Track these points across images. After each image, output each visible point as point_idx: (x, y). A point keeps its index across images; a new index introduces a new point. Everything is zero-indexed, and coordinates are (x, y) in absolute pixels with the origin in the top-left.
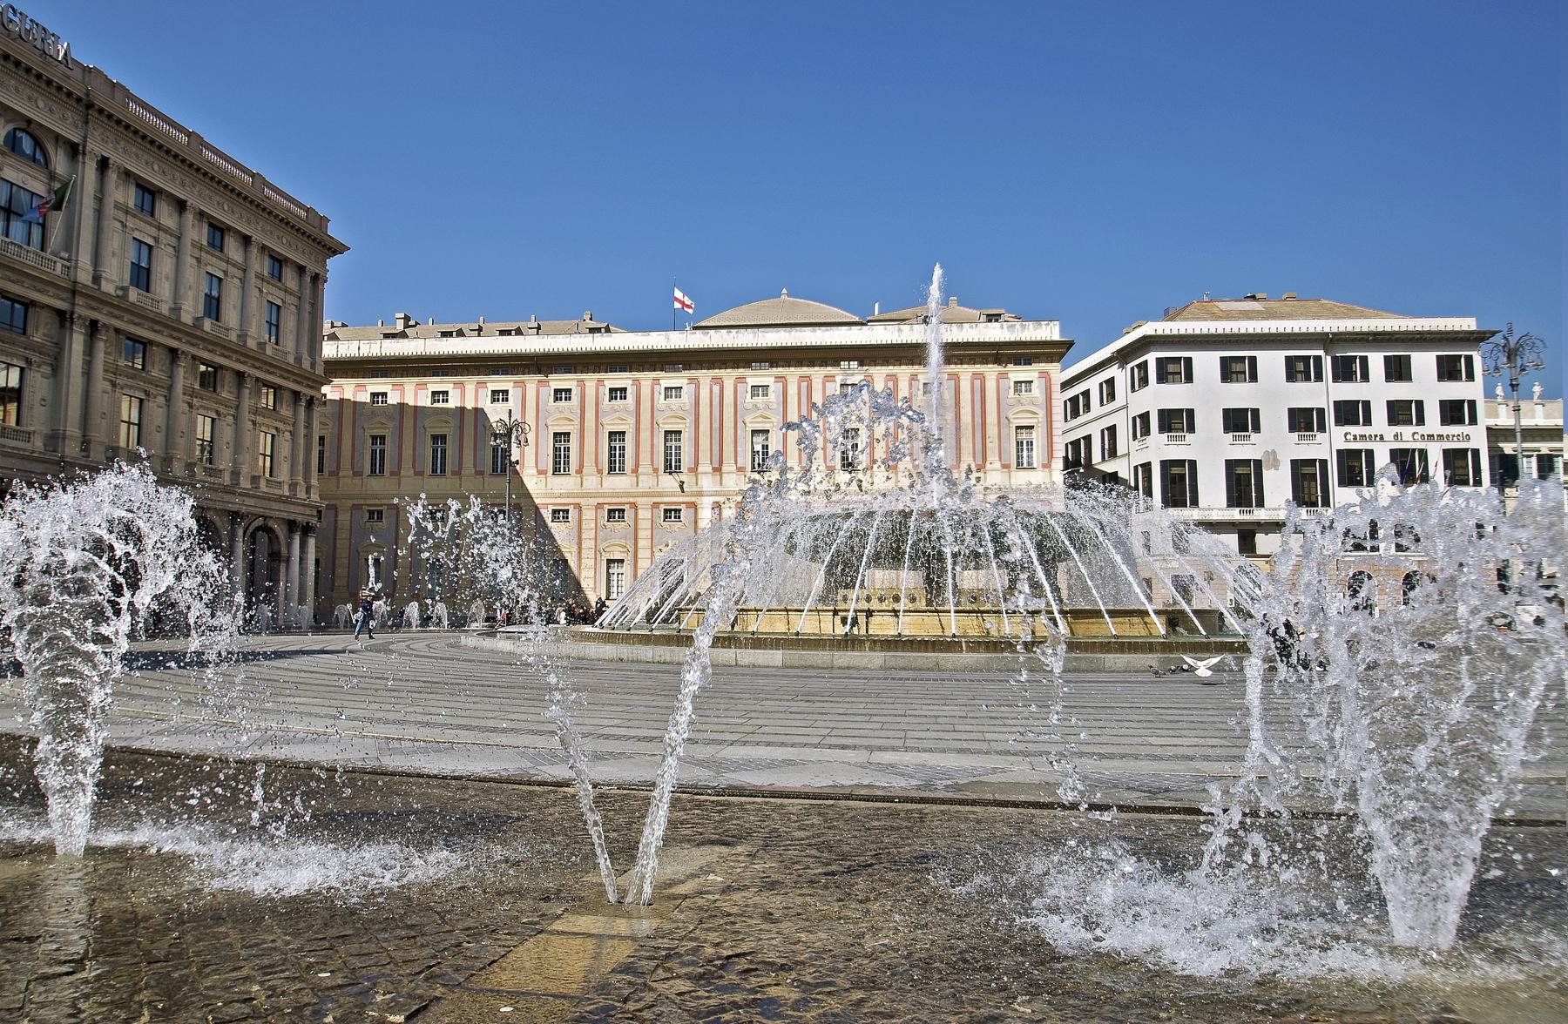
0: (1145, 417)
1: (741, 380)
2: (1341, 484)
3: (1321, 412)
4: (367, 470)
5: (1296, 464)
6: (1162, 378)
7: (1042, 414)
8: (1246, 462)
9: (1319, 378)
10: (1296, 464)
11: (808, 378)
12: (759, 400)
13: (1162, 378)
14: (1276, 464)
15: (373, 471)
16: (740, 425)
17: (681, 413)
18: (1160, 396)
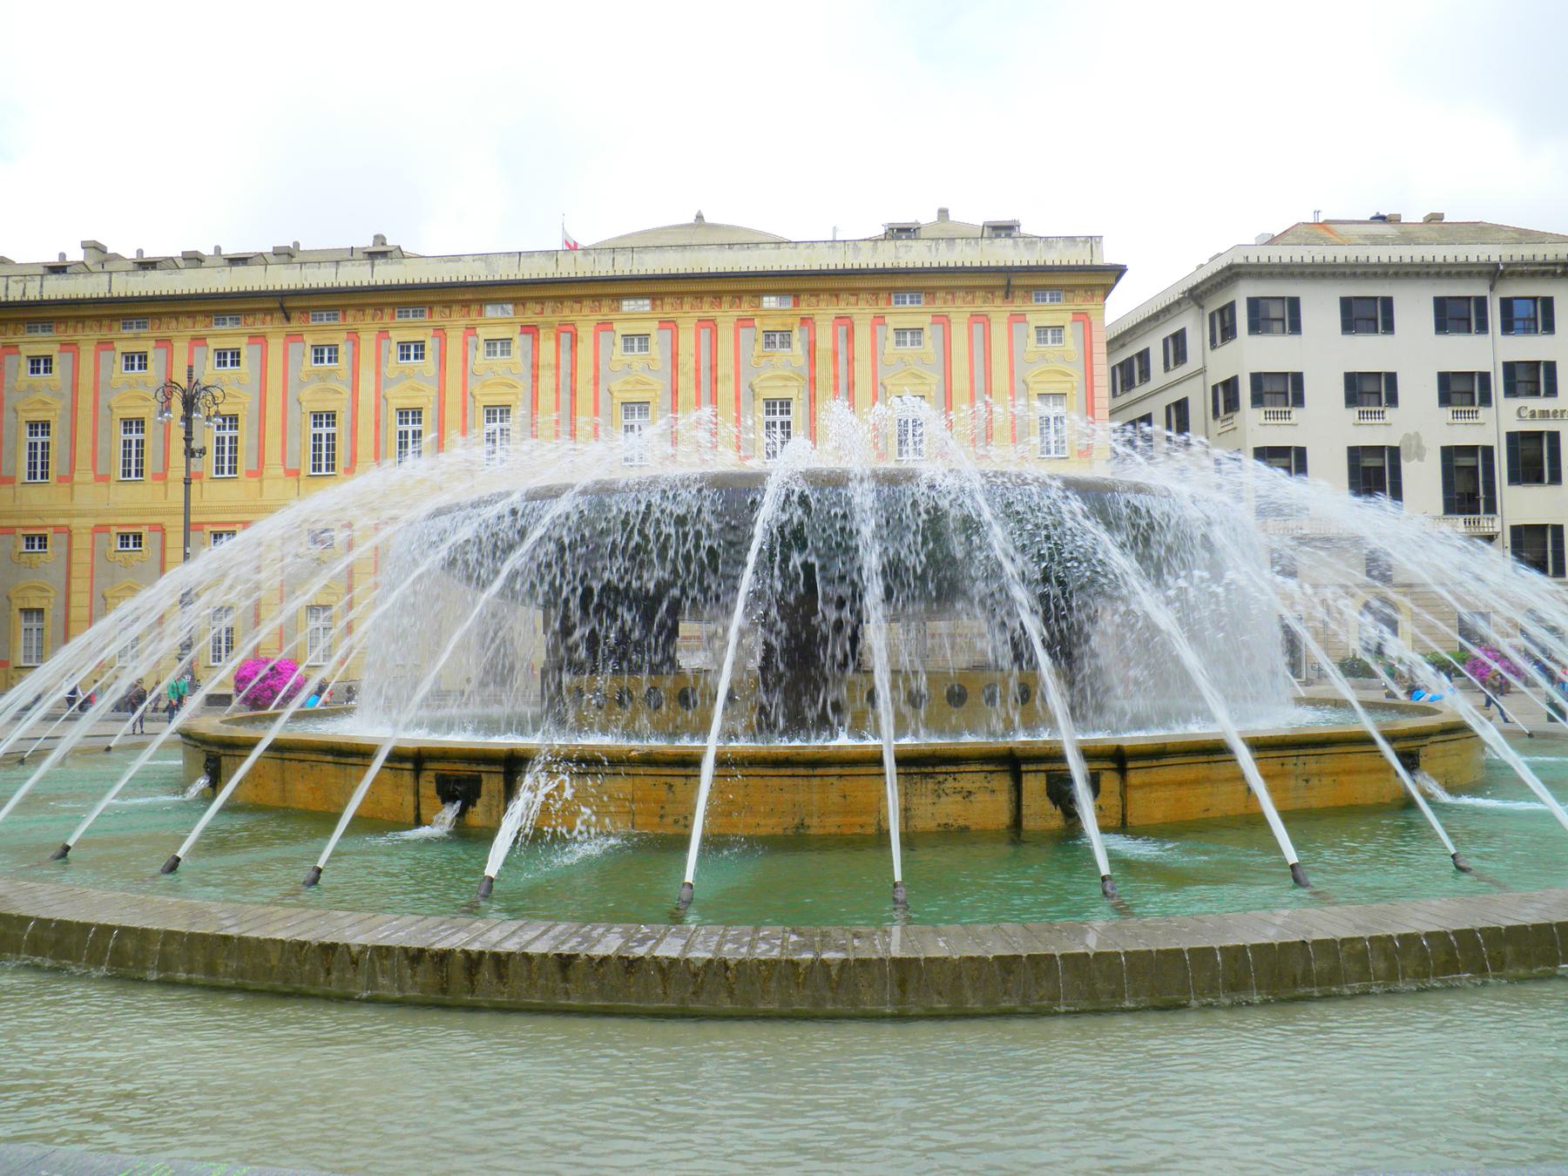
0: (1230, 386)
1: (606, 325)
2: (1514, 479)
3: (1485, 377)
4: (23, 473)
5: (1449, 453)
6: (1255, 327)
7: (1078, 376)
8: (1379, 451)
9: (1483, 327)
10: (1449, 453)
11: (711, 324)
12: (636, 357)
13: (1255, 327)
14: (1420, 454)
15: (32, 475)
18: (1253, 353)
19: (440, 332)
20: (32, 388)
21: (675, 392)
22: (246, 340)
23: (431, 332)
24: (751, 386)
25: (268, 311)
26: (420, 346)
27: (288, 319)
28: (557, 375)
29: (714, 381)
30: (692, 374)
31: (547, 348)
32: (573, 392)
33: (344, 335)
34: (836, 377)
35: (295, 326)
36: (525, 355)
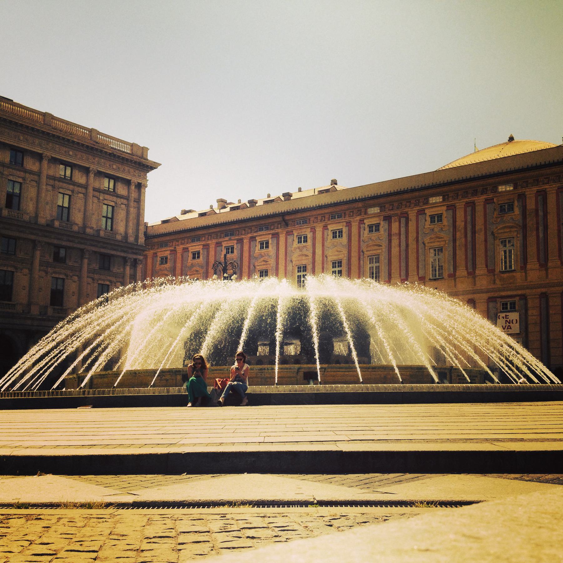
16: (421, 245)
17: (378, 242)
19: (349, 225)
20: (192, 265)
21: (454, 241)
22: (270, 236)
23: (345, 224)
24: (493, 233)
25: (279, 223)
26: (341, 232)
27: (287, 225)
28: (400, 239)
29: (474, 232)
30: (463, 231)
31: (395, 226)
32: (407, 246)
33: (309, 230)
34: (537, 223)
35: (290, 228)
36: (385, 230)
